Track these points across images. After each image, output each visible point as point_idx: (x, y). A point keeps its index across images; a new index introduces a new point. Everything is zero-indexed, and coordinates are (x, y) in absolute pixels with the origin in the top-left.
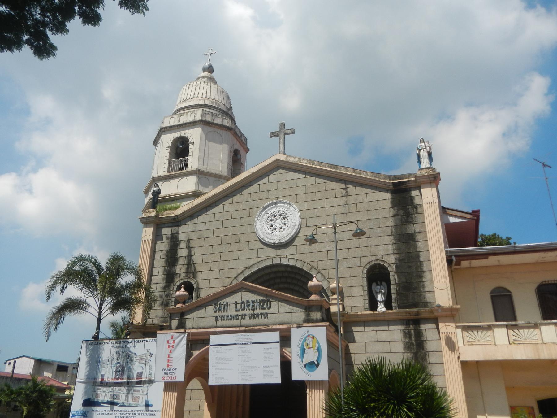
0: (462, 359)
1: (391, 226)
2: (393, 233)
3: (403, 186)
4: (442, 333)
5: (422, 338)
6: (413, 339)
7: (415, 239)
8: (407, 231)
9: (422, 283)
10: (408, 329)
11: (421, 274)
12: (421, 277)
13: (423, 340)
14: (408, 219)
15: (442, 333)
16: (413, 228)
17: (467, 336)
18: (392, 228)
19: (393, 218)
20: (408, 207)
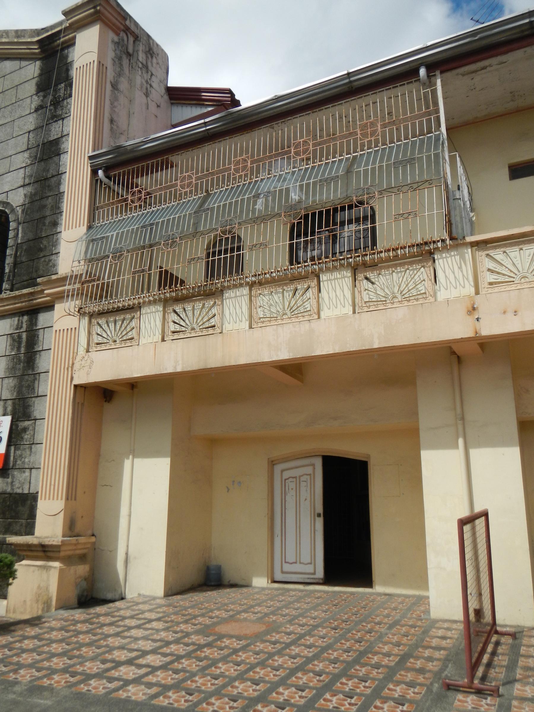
0: (76, 382)
1: (29, 132)
2: (30, 146)
3: (56, 43)
4: (56, 331)
5: (35, 347)
6: (23, 350)
7: (60, 149)
8: (50, 136)
9: (55, 237)
10: (18, 331)
11: (58, 218)
12: (55, 224)
13: (36, 350)
14: (55, 111)
15: (56, 331)
16: (61, 128)
17: (98, 334)
18: (31, 134)
19: (35, 115)
20: (59, 87)
